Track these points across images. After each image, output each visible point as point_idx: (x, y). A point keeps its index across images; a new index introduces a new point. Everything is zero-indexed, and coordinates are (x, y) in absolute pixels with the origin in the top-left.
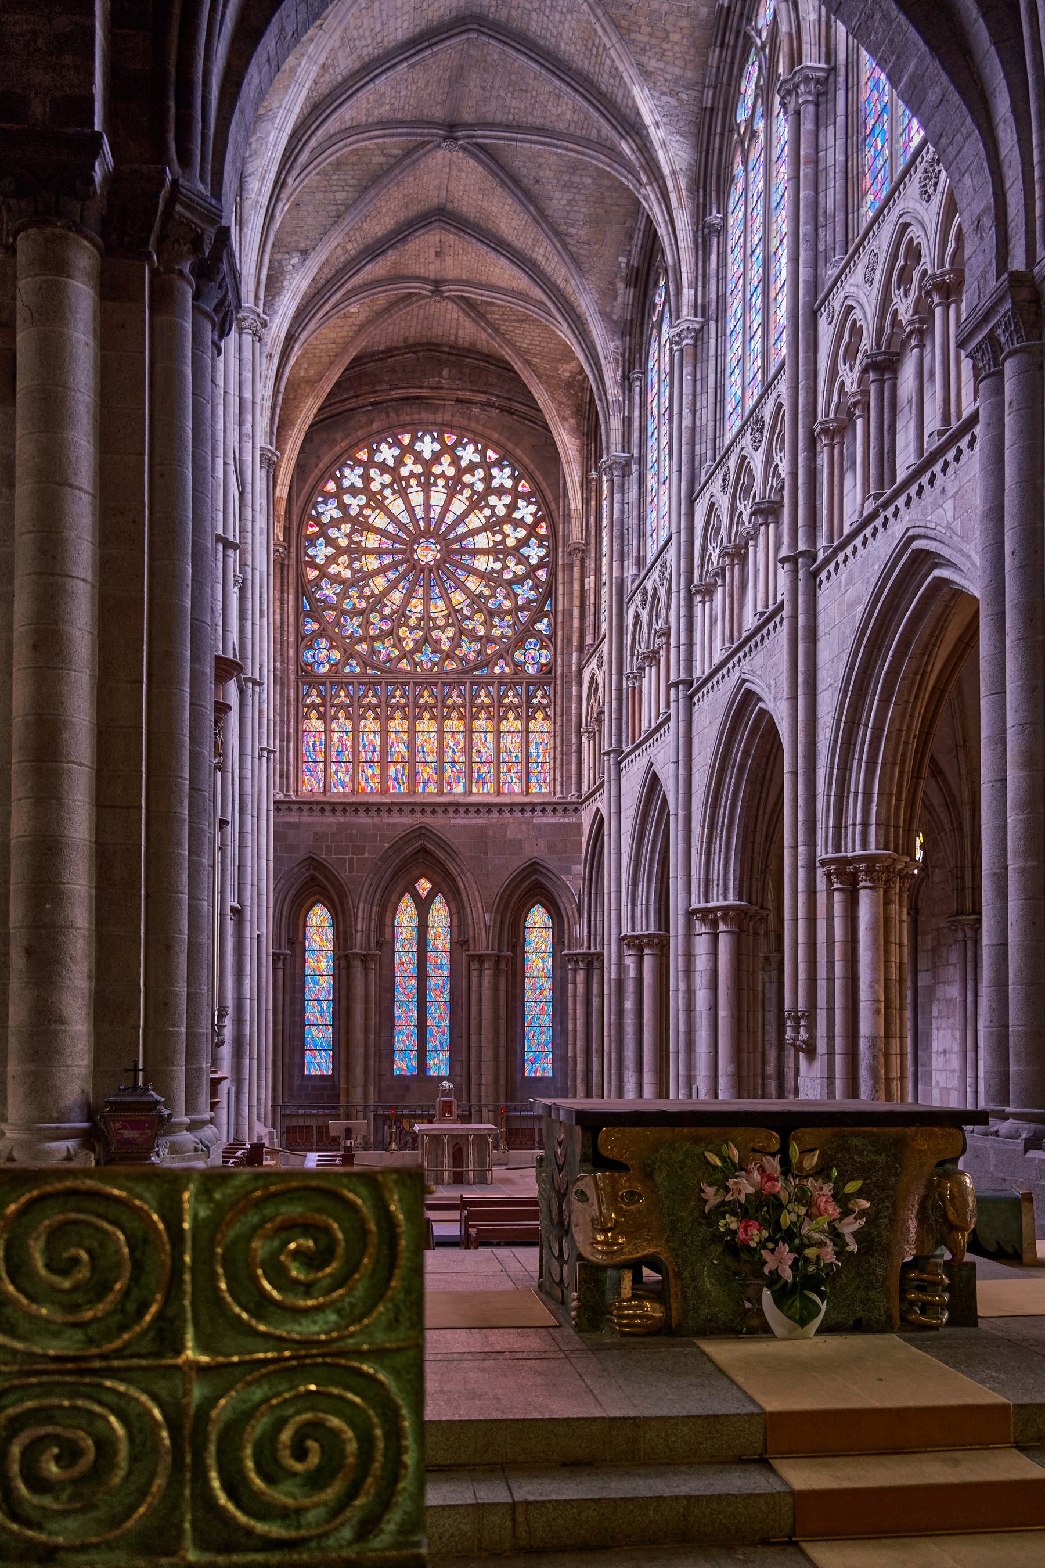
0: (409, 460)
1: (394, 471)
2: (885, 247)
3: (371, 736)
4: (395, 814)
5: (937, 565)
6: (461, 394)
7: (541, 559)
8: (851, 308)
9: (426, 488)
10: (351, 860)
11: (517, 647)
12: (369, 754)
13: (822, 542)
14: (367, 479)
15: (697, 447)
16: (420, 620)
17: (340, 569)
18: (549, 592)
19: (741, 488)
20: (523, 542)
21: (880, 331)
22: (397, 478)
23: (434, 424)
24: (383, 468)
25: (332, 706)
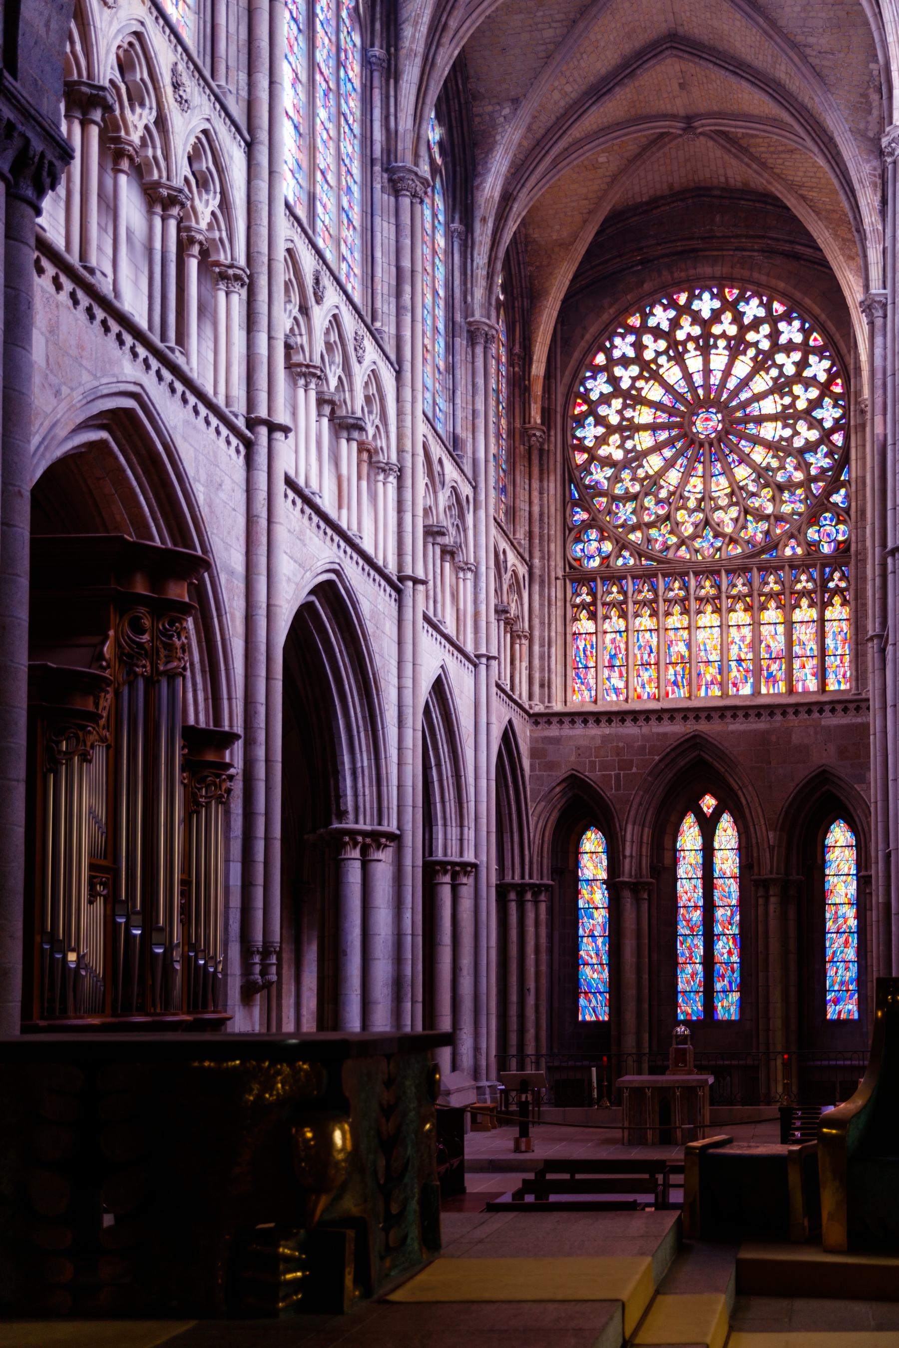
0: (686, 321)
1: (669, 336)
3: (648, 635)
7: (837, 421)
9: (705, 351)
10: (618, 776)
11: (811, 523)
12: (646, 657)
14: (639, 347)
17: (613, 450)
18: (843, 462)
20: (816, 404)
22: (673, 343)
23: (713, 278)
24: (657, 333)
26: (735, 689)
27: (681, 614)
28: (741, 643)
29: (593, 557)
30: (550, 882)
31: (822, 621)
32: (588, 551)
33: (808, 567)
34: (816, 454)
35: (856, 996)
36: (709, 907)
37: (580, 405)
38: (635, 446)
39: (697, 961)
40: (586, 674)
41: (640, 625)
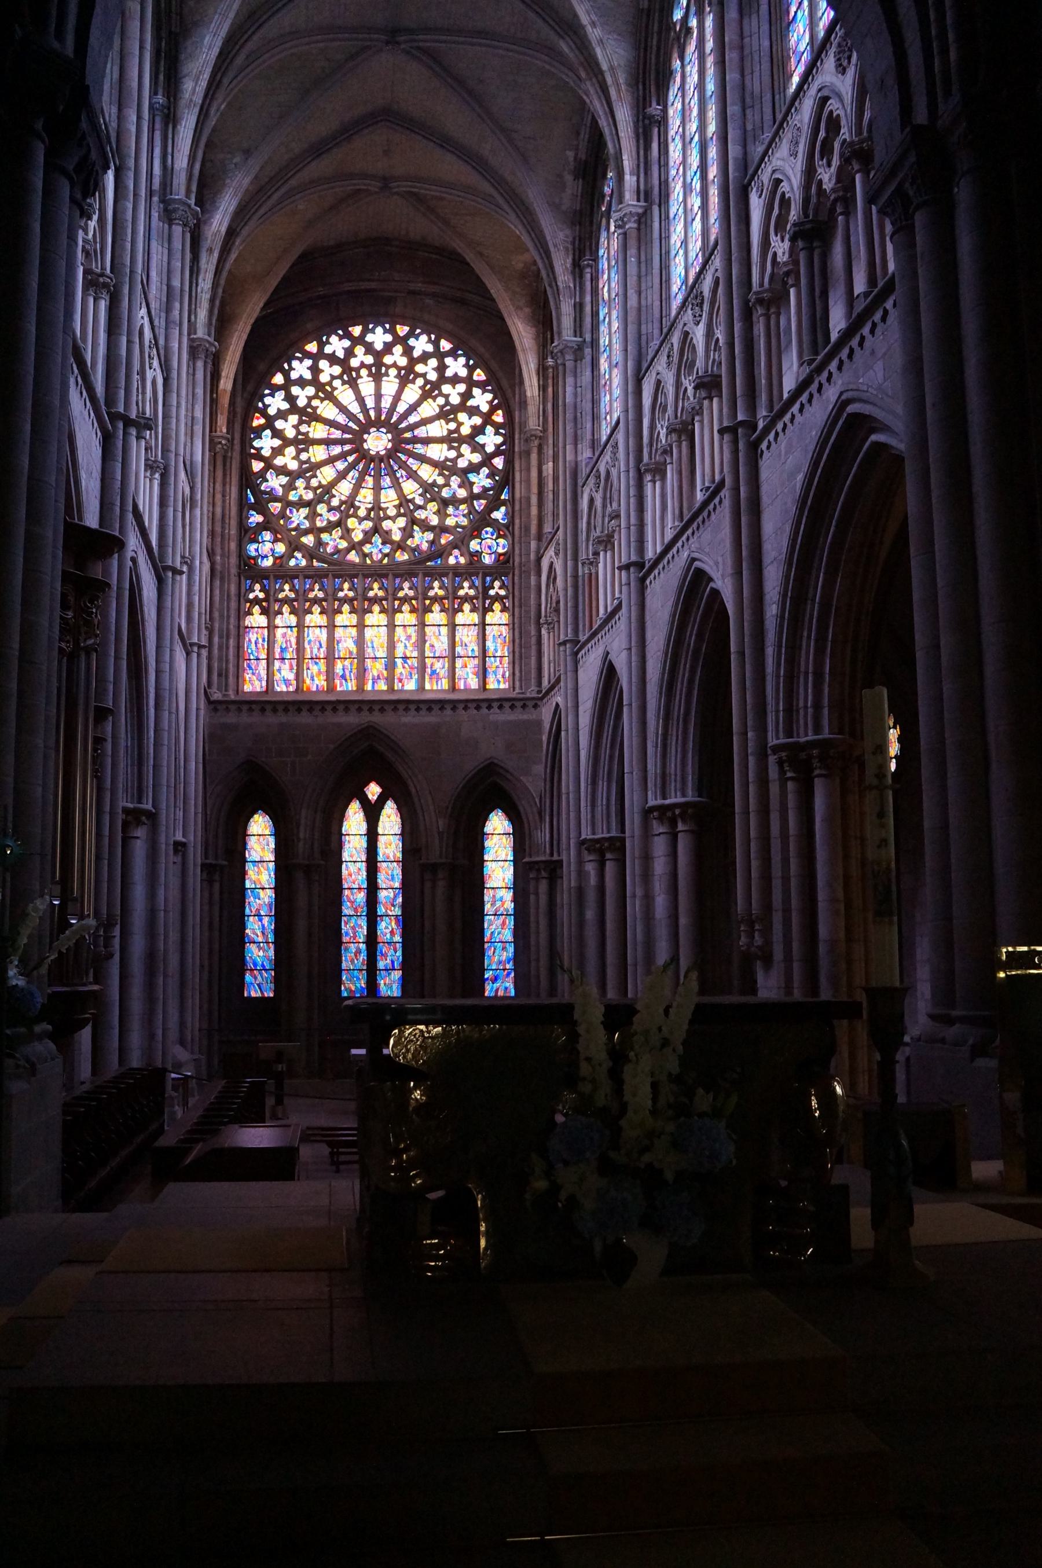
2: (806, 119)
4: (341, 713)
5: (873, 430)
6: (412, 286)
7: (498, 447)
8: (778, 181)
9: (377, 377)
11: (473, 537)
12: (315, 651)
13: (762, 412)
14: (315, 370)
15: (643, 327)
16: (369, 510)
17: (288, 459)
19: (684, 363)
20: (478, 430)
21: (806, 200)
22: (347, 369)
24: (333, 359)
25: (277, 600)
26: (400, 684)
27: (350, 613)
28: (407, 642)
29: (266, 556)
30: (225, 863)
31: (483, 625)
32: (262, 551)
33: (471, 575)
34: (478, 474)
35: (513, 975)
36: (372, 888)
37: (258, 418)
38: (309, 458)
39: (361, 941)
40: (258, 665)
41: (311, 621)
